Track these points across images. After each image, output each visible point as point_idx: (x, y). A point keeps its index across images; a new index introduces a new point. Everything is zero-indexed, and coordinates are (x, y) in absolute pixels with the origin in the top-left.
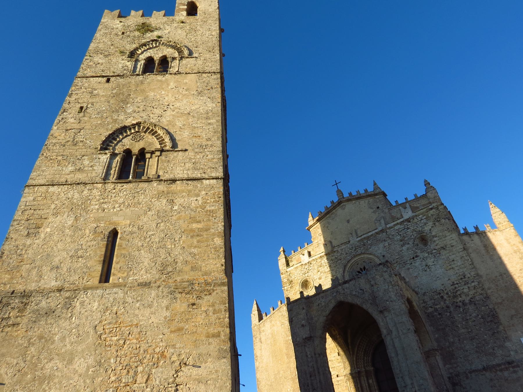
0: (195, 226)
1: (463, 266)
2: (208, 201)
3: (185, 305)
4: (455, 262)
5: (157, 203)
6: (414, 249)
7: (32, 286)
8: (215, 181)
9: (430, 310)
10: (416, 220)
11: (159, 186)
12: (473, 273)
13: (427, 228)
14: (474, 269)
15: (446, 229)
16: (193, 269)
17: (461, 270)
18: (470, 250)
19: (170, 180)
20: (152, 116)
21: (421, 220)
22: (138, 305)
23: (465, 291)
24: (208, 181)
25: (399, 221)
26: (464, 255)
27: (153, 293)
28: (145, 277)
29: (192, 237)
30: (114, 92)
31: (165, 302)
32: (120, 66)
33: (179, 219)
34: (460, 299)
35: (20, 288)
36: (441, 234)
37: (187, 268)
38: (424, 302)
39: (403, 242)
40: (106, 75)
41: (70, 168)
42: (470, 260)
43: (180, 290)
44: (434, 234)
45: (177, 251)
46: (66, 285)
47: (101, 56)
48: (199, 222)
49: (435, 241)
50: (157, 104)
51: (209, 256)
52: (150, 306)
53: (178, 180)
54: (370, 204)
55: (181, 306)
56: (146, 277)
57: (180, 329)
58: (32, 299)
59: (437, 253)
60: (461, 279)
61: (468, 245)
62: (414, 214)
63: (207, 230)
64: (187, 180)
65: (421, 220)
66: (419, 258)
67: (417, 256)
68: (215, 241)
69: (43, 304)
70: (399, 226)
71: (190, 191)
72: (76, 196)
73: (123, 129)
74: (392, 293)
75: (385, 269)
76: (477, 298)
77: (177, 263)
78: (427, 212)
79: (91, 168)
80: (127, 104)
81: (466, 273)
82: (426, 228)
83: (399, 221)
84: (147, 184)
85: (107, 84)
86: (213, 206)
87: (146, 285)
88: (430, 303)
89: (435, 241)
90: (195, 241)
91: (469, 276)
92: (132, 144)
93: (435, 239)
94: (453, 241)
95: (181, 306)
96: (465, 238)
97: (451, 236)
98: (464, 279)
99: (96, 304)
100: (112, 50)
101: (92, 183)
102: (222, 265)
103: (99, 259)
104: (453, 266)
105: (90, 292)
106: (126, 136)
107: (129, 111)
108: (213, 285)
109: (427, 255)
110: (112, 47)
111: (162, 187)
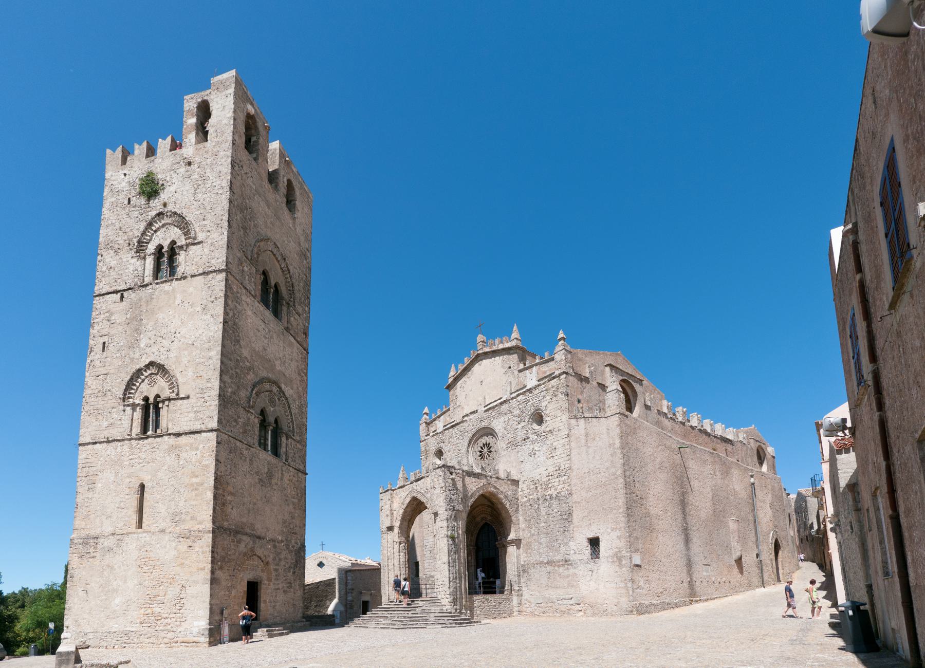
3: (186, 547)
5: (168, 458)
9: (525, 499)
16: (193, 518)
20: (162, 349)
23: (556, 484)
27: (167, 537)
30: (128, 316)
31: (174, 544)
32: (131, 268)
34: (549, 492)
37: (188, 518)
38: (522, 491)
45: (181, 504)
52: (165, 547)
55: (183, 547)
56: (163, 525)
57: (182, 564)
73: (139, 372)
76: (562, 494)
87: (163, 531)
88: (526, 492)
95: (183, 547)
106: (143, 381)
107: (142, 345)
111: (172, 440)
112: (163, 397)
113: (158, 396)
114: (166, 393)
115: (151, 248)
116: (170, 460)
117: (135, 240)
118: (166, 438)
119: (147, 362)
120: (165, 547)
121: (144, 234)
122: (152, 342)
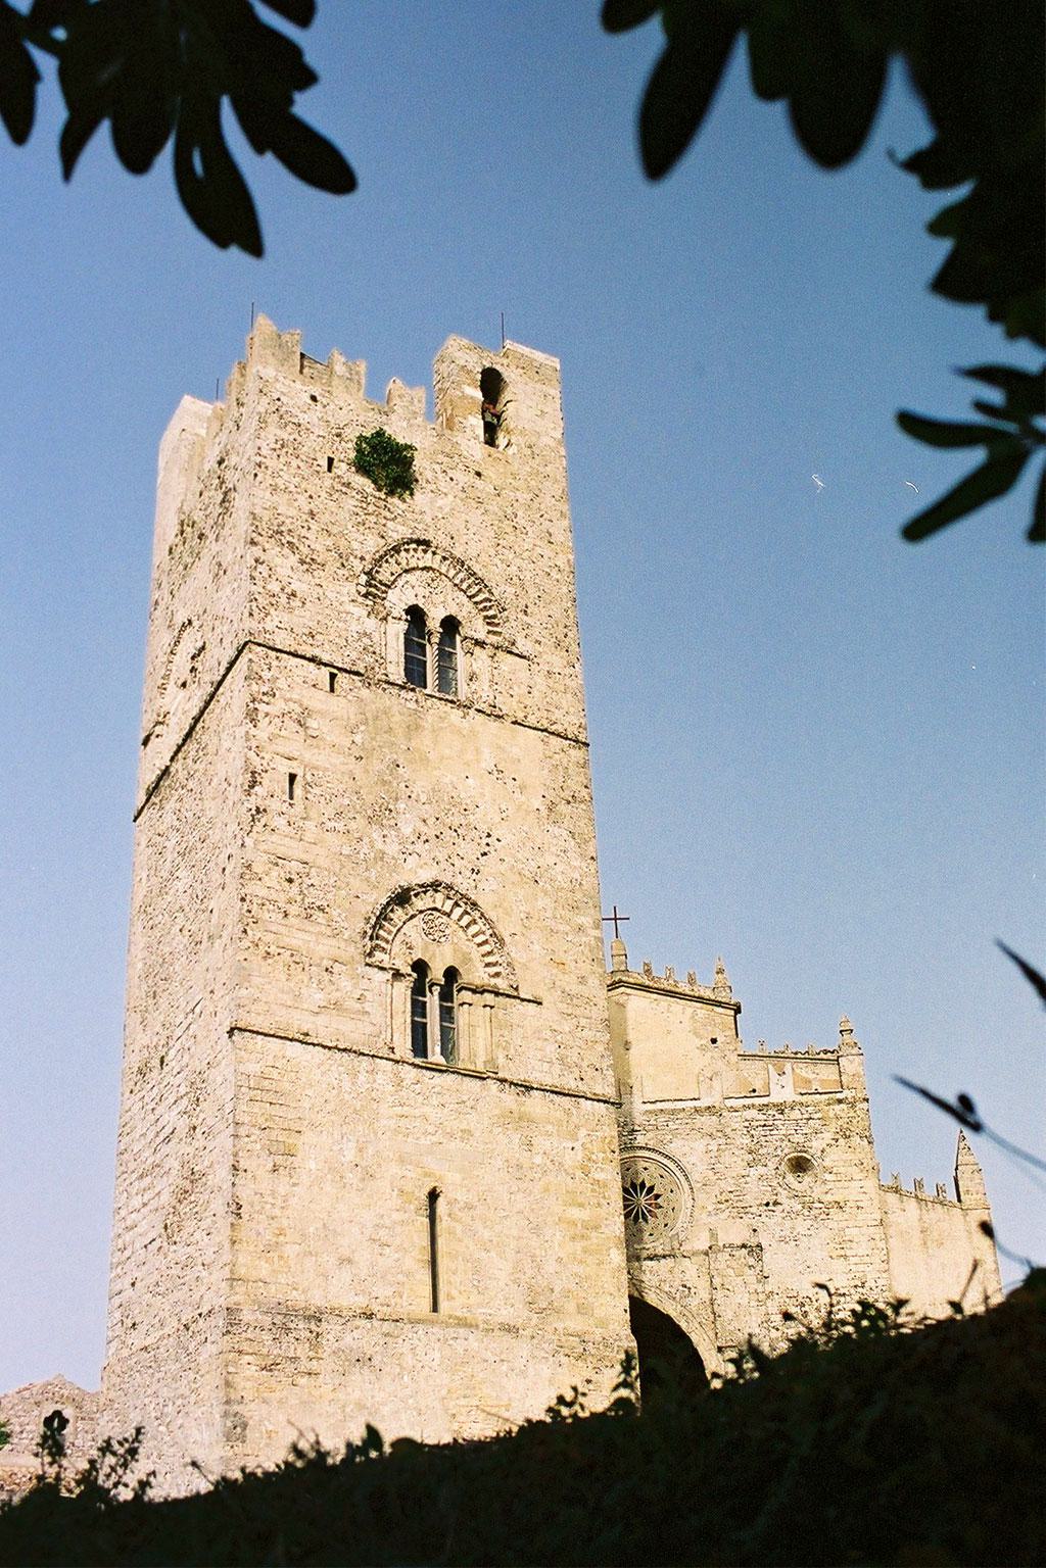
0: (575, 1213)
1: (867, 1259)
2: (594, 1157)
4: (854, 1245)
6: (774, 1184)
7: (317, 1300)
8: (602, 1104)
10: (796, 1114)
11: (502, 1095)
12: (881, 1282)
13: (816, 1145)
14: (884, 1275)
15: (857, 1162)
16: (581, 1309)
17: (861, 1268)
18: (891, 1231)
19: (521, 1086)
21: (808, 1119)
22: (504, 1368)
24: (590, 1102)
25: (757, 1101)
26: (877, 1237)
28: (505, 1312)
29: (573, 1238)
30: (358, 738)
31: (546, 1372)
32: (354, 627)
33: (546, 1190)
35: (297, 1298)
36: (842, 1170)
37: (571, 1307)
39: (754, 1157)
40: (326, 658)
41: (320, 998)
42: (885, 1252)
43: (567, 1351)
44: (828, 1163)
45: (550, 1267)
46: (375, 1308)
47: (294, 559)
48: (581, 1205)
49: (825, 1182)
50: (464, 822)
51: (602, 1287)
53: (537, 1089)
54: (696, 1021)
56: (506, 1315)
58: (324, 1324)
59: (819, 1210)
60: (856, 1286)
61: (891, 1217)
62: (799, 1098)
63: (596, 1228)
64: (552, 1092)
65: (808, 1119)
66: (780, 1208)
67: (776, 1203)
68: (612, 1256)
69: (348, 1339)
70: (753, 1113)
71: (559, 1123)
72: (347, 1085)
73: (402, 898)
74: (754, 1319)
75: (751, 1261)
77: (552, 1290)
78: (829, 1104)
79: (358, 1006)
80: (397, 799)
81: (869, 1277)
82: (814, 1144)
83: (757, 1101)
84: (479, 1083)
85: (332, 698)
86: (602, 1170)
87: (510, 1329)
89: (825, 1182)
90: (579, 1246)
91: (873, 1285)
92: (426, 948)
93: (828, 1177)
94: (862, 1197)
96: (892, 1198)
97: (862, 1183)
98: (859, 1290)
99: (437, 1355)
100: (319, 544)
101: (373, 1056)
102: (626, 1311)
103: (420, 1256)
104: (848, 1253)
105: (420, 1327)
108: (616, 1349)
109: (800, 1207)
110: (314, 526)
111: (510, 1097)
112: (465, 978)
113: (451, 974)
114: (475, 973)
115: (398, 600)
116: (508, 1144)
117: (358, 566)
118: (493, 1086)
119: (426, 876)
120: (523, 1373)
121: (379, 560)
122: (431, 832)
